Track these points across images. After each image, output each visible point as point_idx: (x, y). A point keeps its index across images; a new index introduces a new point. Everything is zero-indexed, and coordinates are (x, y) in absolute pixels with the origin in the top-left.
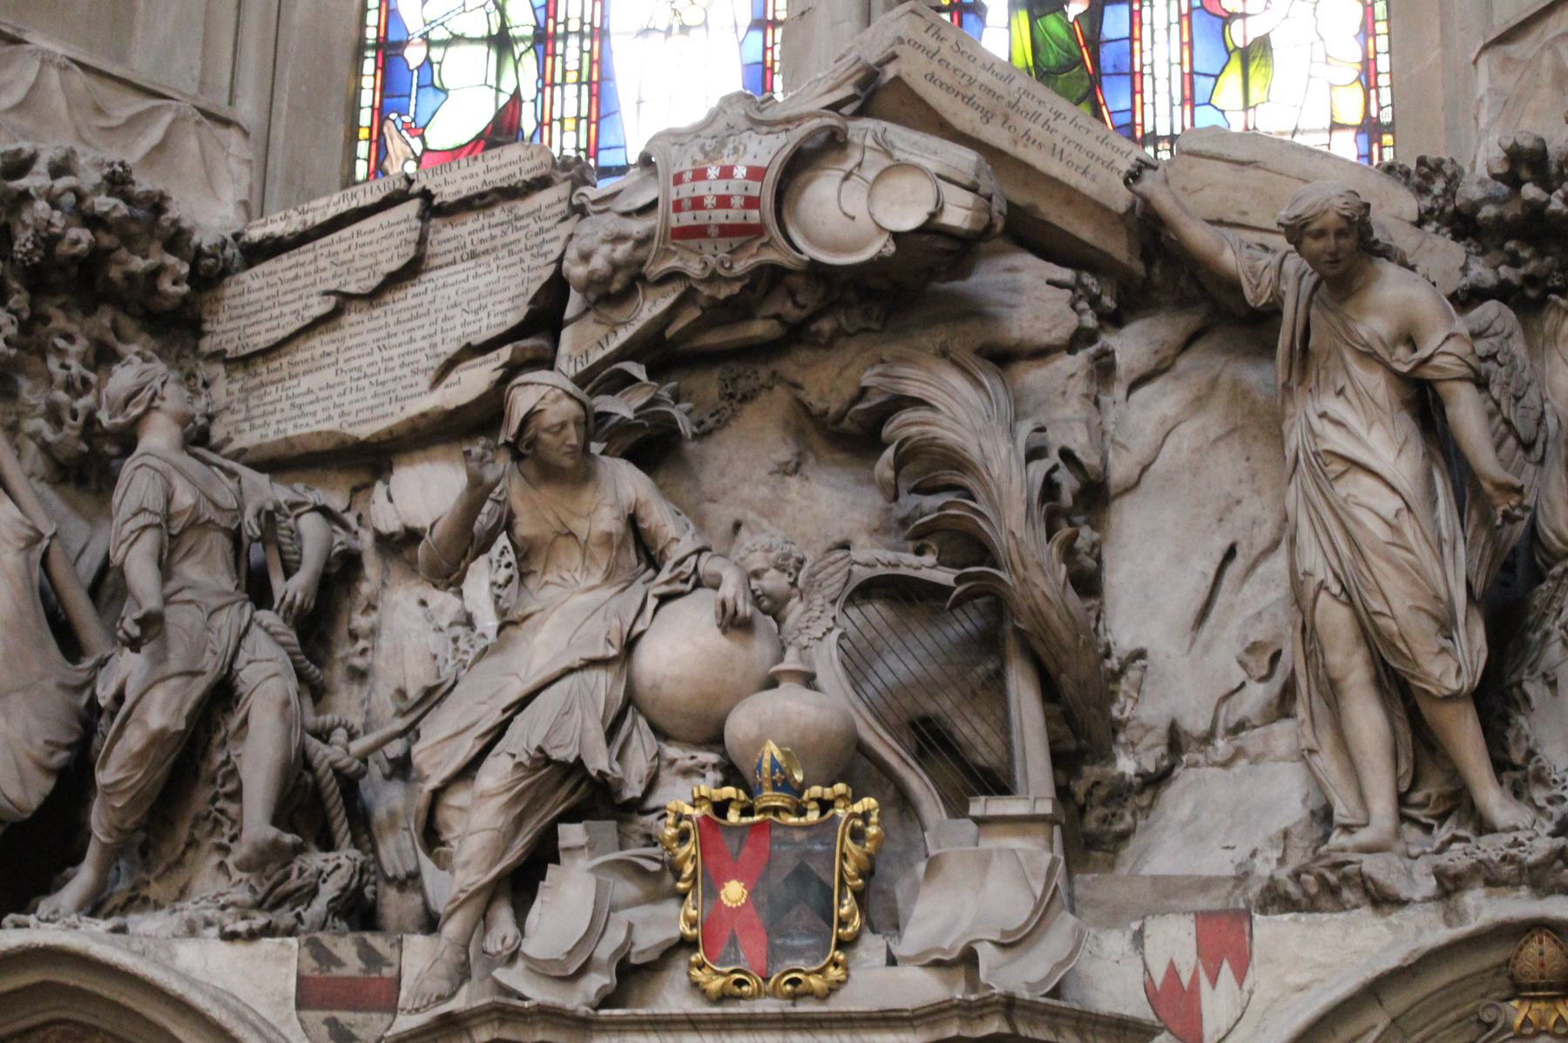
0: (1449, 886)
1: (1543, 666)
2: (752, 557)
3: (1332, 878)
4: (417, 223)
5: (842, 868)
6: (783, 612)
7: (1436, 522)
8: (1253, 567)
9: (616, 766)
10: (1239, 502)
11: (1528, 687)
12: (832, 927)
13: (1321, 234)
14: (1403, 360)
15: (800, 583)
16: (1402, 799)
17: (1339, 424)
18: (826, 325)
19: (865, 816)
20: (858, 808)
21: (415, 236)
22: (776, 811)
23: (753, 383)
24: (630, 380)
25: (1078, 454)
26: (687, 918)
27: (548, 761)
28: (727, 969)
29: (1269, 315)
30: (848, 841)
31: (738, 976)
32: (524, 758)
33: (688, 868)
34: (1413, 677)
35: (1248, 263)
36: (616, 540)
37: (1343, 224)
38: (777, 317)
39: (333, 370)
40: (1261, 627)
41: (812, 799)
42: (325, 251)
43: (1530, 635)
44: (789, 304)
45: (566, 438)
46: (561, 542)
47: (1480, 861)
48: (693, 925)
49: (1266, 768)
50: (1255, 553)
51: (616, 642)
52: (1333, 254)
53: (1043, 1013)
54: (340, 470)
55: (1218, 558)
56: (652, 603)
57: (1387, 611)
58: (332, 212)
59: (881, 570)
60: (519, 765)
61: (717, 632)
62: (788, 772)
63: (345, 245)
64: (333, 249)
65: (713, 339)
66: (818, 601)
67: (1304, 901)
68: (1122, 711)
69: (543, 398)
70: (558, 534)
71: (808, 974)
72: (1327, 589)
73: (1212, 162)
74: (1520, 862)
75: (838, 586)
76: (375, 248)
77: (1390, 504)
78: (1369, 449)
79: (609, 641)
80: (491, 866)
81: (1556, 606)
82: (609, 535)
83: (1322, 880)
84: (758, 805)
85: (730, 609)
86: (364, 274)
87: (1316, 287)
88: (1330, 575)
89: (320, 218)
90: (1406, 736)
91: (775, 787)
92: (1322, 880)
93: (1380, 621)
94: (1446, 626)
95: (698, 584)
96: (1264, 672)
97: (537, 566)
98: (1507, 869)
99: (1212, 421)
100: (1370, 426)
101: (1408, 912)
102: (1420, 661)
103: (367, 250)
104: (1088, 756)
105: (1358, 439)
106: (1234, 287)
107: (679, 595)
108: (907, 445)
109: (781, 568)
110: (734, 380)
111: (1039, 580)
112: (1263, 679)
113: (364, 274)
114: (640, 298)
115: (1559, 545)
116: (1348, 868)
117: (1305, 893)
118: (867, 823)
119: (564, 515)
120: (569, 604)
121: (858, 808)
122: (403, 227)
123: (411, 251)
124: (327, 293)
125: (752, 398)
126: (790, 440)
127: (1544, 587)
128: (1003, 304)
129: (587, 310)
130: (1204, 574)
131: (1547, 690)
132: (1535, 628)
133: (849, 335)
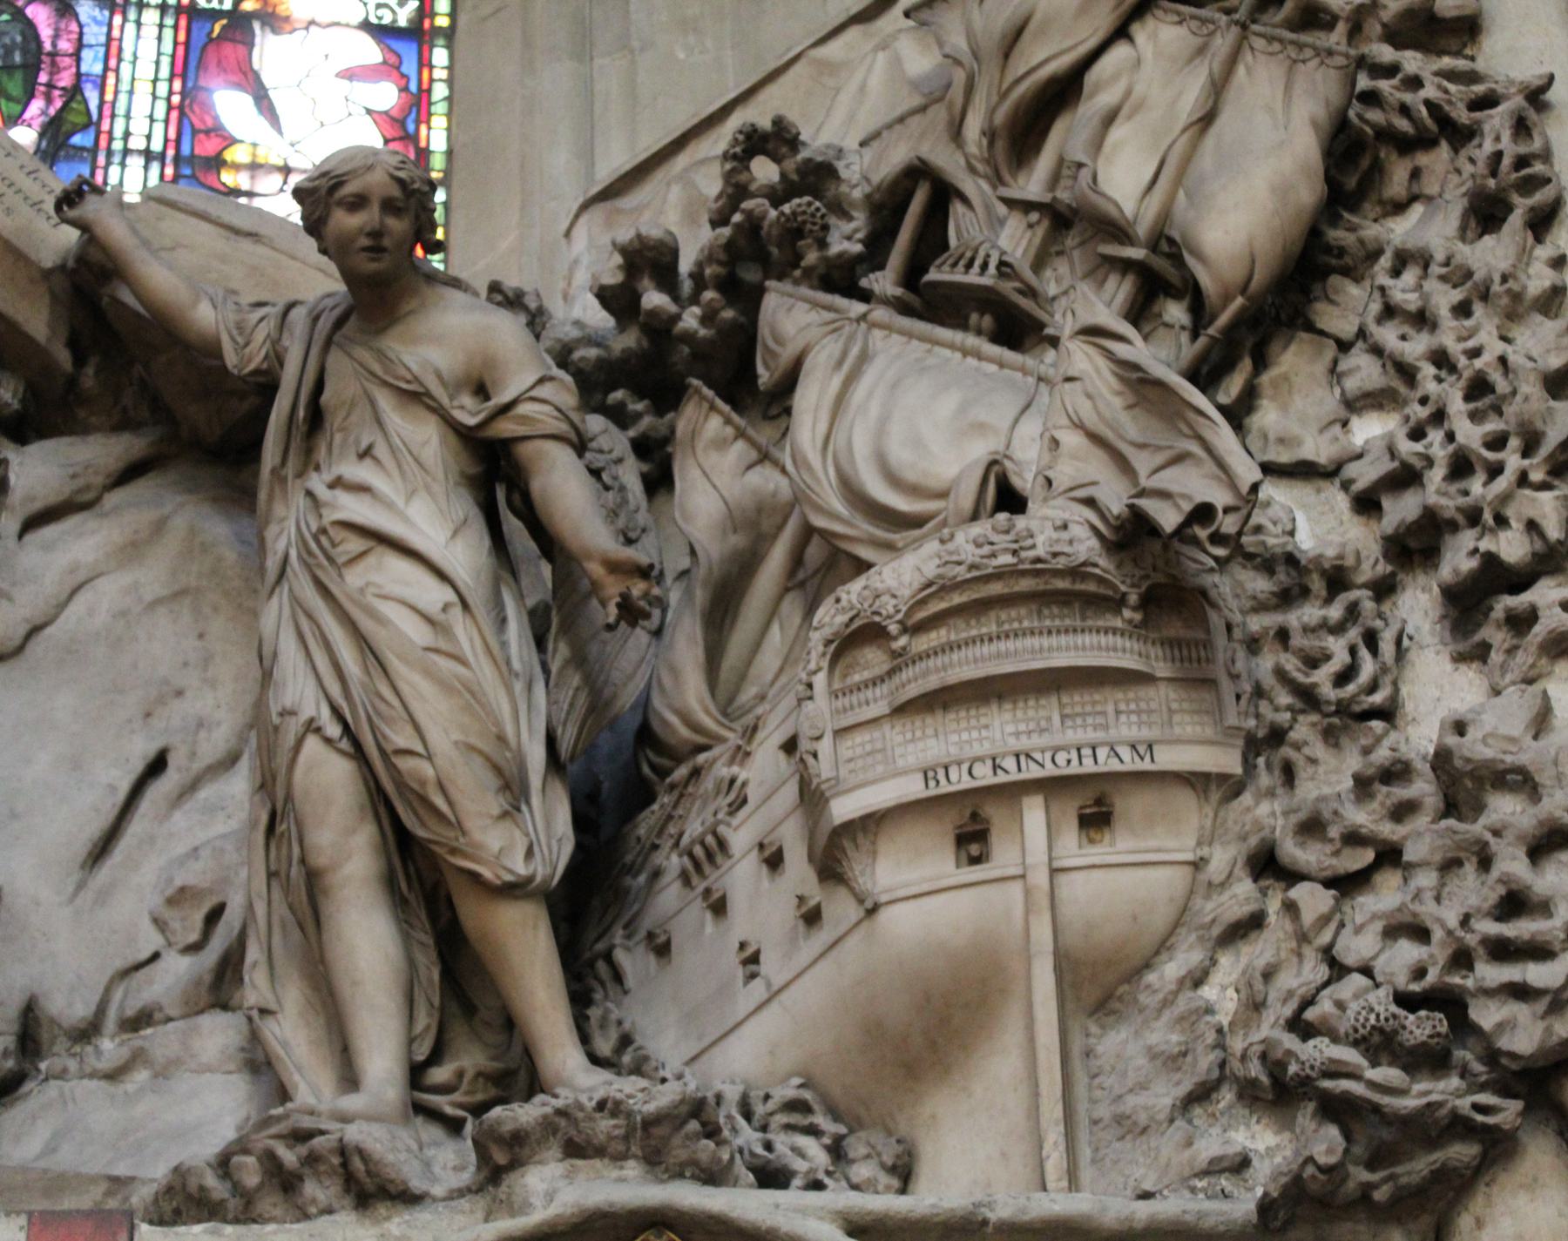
0: (501, 1158)
1: (647, 923)
3: (289, 1157)
7: (504, 645)
8: (193, 786)
10: (179, 693)
11: (620, 956)
13: (358, 202)
14: (469, 412)
16: (416, 1074)
17: (362, 489)
29: (265, 385)
34: (454, 851)
35: (232, 317)
37: (396, 192)
40: (197, 866)
43: (628, 881)
47: (560, 1112)
49: (183, 1082)
50: (198, 766)
52: (376, 234)
55: (138, 766)
57: (420, 749)
67: (234, 1204)
72: (318, 730)
73: (193, 221)
74: (629, 1114)
77: (433, 595)
78: (406, 520)
81: (672, 829)
83: (270, 1162)
87: (340, 323)
88: (325, 712)
90: (432, 973)
92: (270, 1162)
93: (404, 764)
94: (513, 788)
96: (194, 937)
98: (605, 1125)
99: (151, 577)
100: (410, 495)
101: (422, 1215)
102: (471, 824)
105: (389, 505)
106: (213, 350)
112: (194, 948)
115: (684, 732)
116: (317, 1142)
117: (237, 1189)
127: (655, 807)
130: (112, 788)
131: (652, 958)
132: (634, 871)
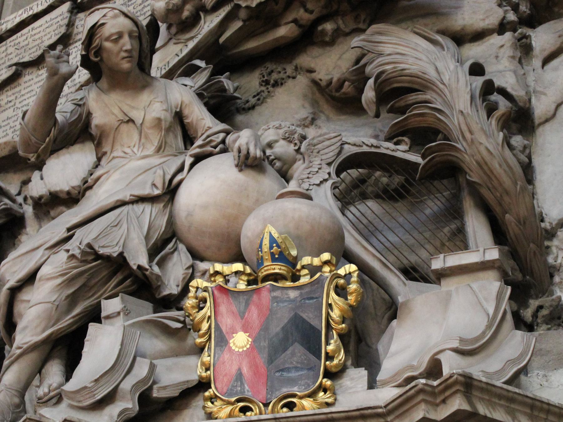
2: (267, 133)
4: (68, 15)
5: (328, 314)
6: (290, 172)
9: (156, 269)
12: (320, 360)
15: (303, 149)
18: (329, 27)
19: (348, 276)
20: (342, 272)
21: (66, 21)
22: (276, 277)
23: (282, 75)
24: (195, 69)
25: (509, 90)
26: (203, 364)
27: (98, 256)
28: (233, 399)
30: (333, 294)
31: (241, 404)
32: (77, 252)
33: (205, 326)
36: (164, 125)
38: (295, 21)
39: (12, 109)
41: (303, 267)
42: (12, 44)
44: (302, 11)
45: (124, 45)
46: (125, 128)
48: (207, 369)
51: (160, 185)
53: (500, 397)
54: (15, 172)
56: (189, 161)
58: (18, 20)
59: (365, 149)
60: (73, 256)
61: (235, 170)
62: (283, 246)
63: (24, 37)
64: (17, 41)
65: (251, 45)
66: (317, 161)
68: (556, 259)
69: (104, 16)
70: (122, 122)
71: (301, 398)
75: (332, 154)
76: (42, 34)
79: (154, 185)
80: (44, 331)
82: (159, 120)
84: (263, 273)
85: (244, 152)
86: (34, 49)
89: (10, 26)
91: (274, 259)
95: (225, 150)
97: (106, 148)
103: (37, 37)
104: (532, 292)
107: (210, 155)
108: (383, 77)
109: (288, 139)
110: (270, 74)
111: (482, 139)
113: (34, 49)
114: (202, 21)
118: (349, 283)
119: (126, 109)
120: (127, 167)
121: (342, 272)
122: (59, 19)
123: (63, 30)
124: (11, 66)
125: (282, 84)
126: (307, 105)
128: (451, 8)
129: (170, 39)
133: (347, 34)
